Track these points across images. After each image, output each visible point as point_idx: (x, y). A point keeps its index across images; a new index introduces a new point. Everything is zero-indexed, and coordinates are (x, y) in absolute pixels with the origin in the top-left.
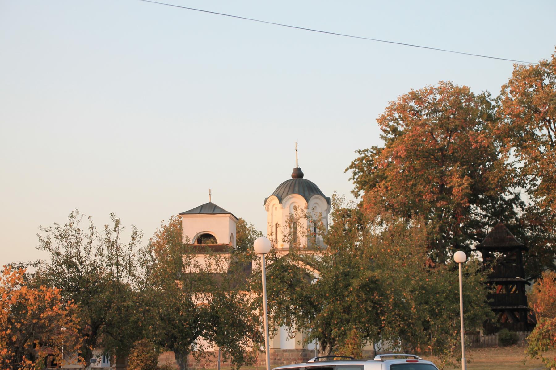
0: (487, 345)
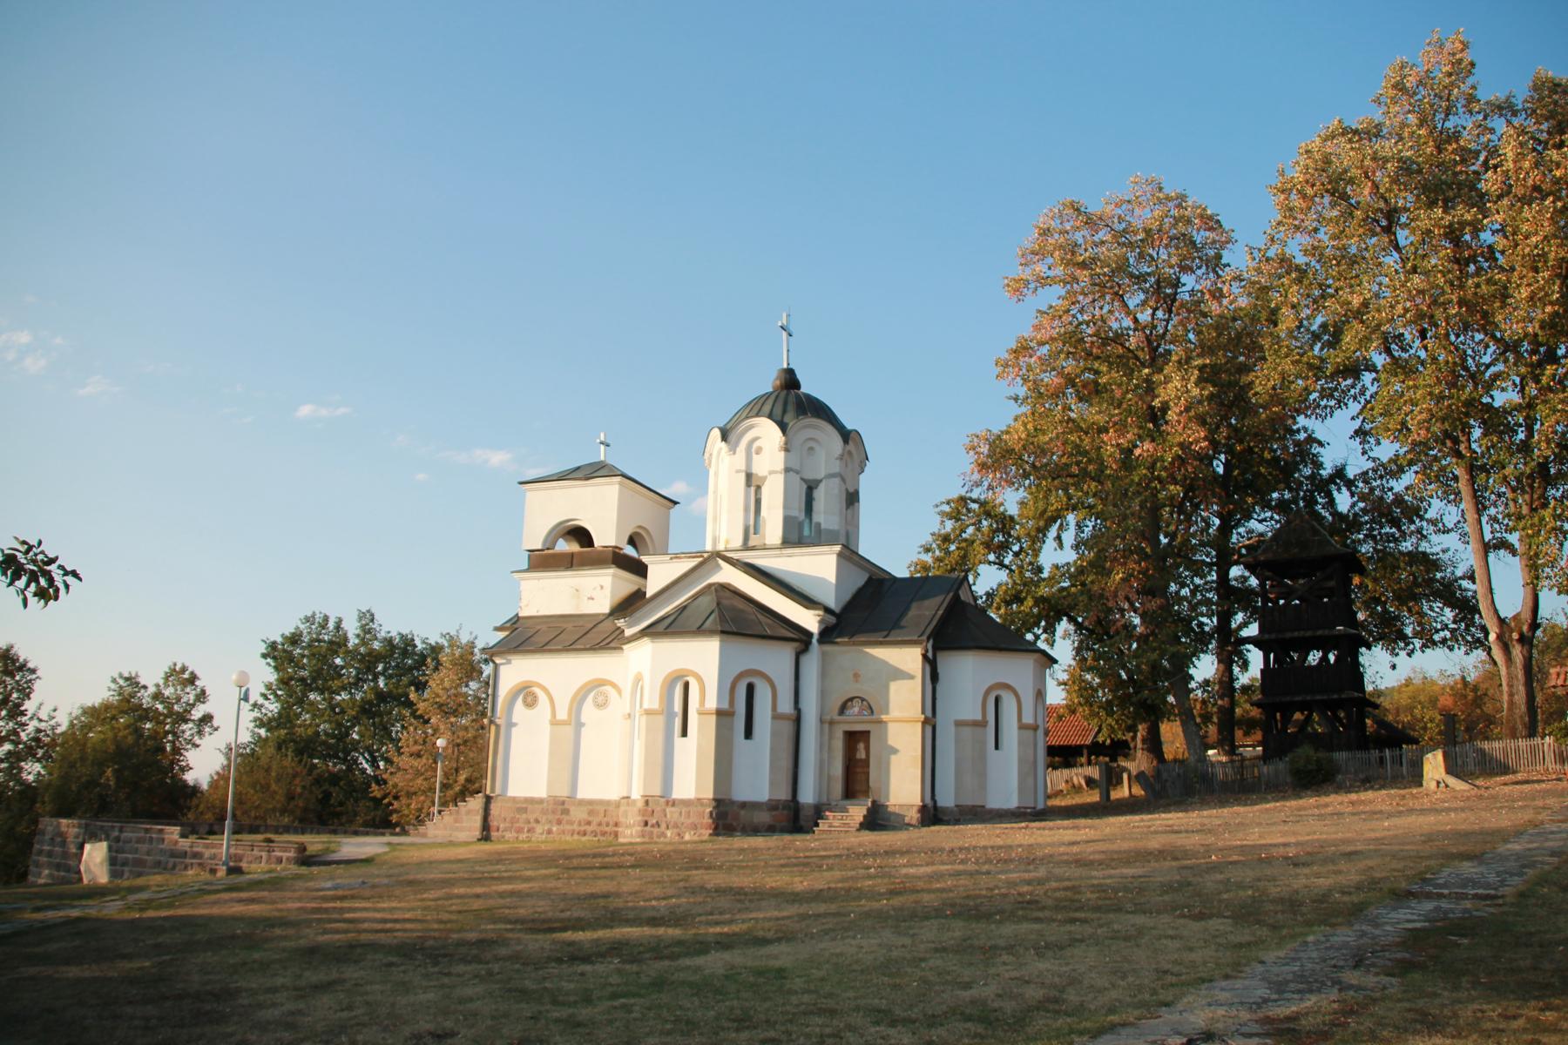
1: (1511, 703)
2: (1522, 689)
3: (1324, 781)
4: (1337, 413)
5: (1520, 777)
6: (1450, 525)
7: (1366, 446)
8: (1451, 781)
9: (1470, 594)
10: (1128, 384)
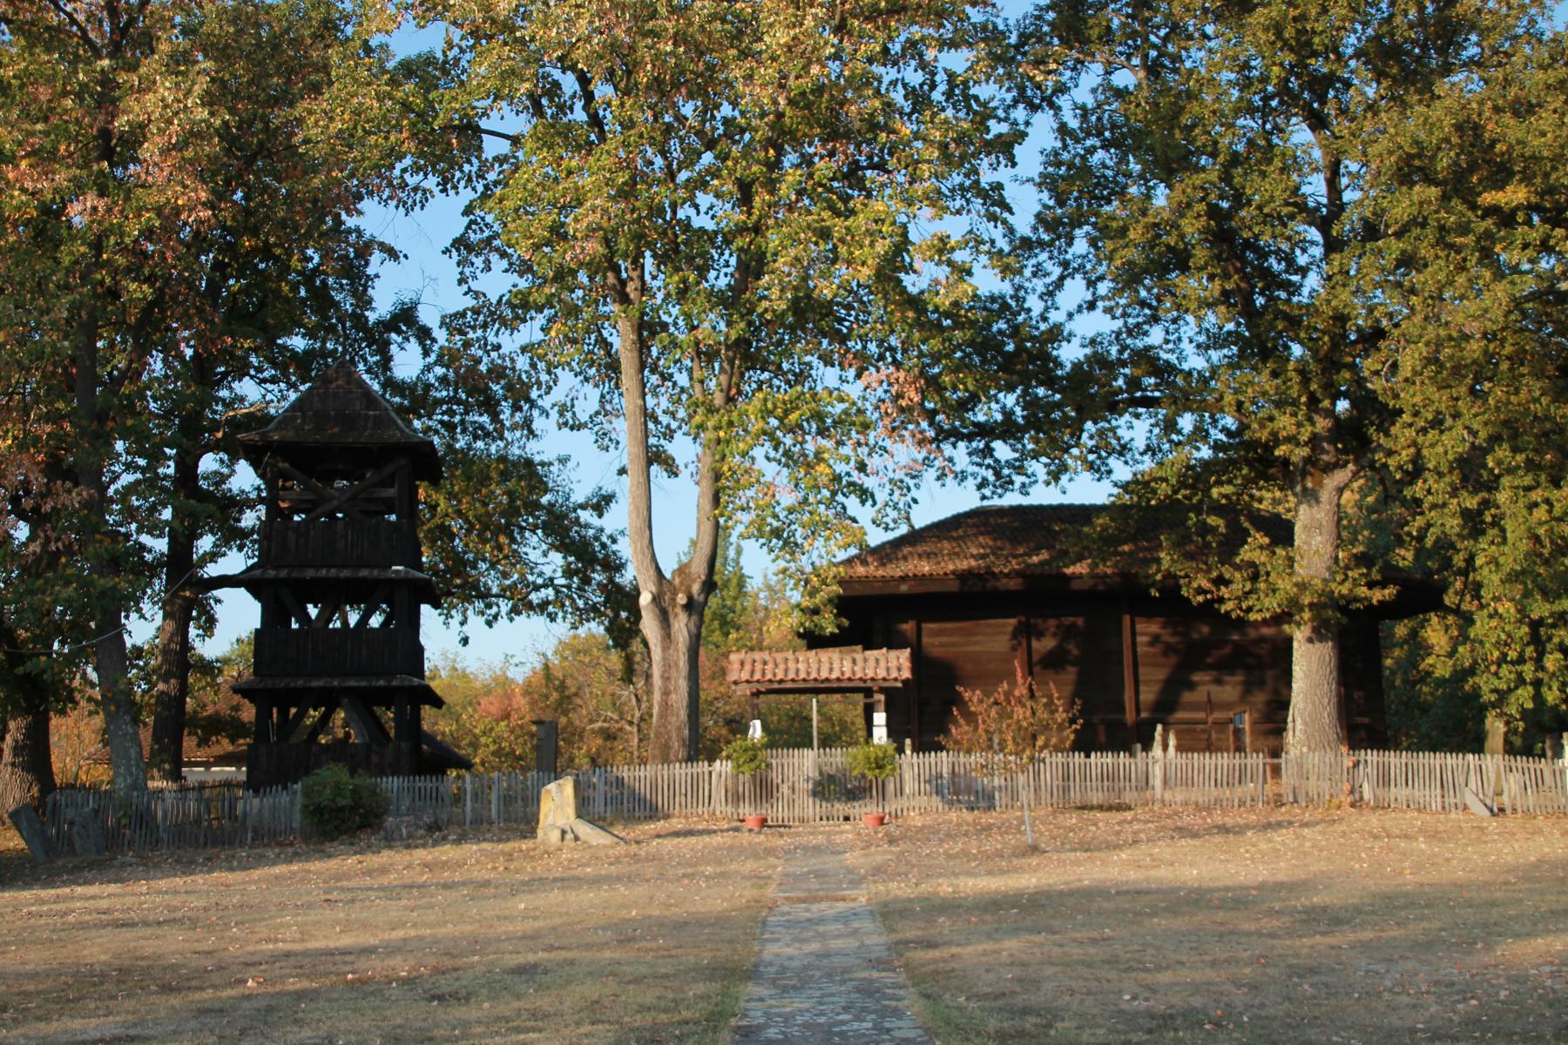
0: (255, 831)
1: (665, 706)
2: (683, 684)
3: (361, 827)
4: (438, 201)
5: (677, 824)
6: (583, 417)
7: (467, 271)
8: (585, 830)
9: (591, 532)
10: (67, 80)
